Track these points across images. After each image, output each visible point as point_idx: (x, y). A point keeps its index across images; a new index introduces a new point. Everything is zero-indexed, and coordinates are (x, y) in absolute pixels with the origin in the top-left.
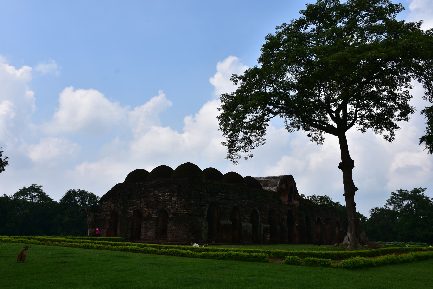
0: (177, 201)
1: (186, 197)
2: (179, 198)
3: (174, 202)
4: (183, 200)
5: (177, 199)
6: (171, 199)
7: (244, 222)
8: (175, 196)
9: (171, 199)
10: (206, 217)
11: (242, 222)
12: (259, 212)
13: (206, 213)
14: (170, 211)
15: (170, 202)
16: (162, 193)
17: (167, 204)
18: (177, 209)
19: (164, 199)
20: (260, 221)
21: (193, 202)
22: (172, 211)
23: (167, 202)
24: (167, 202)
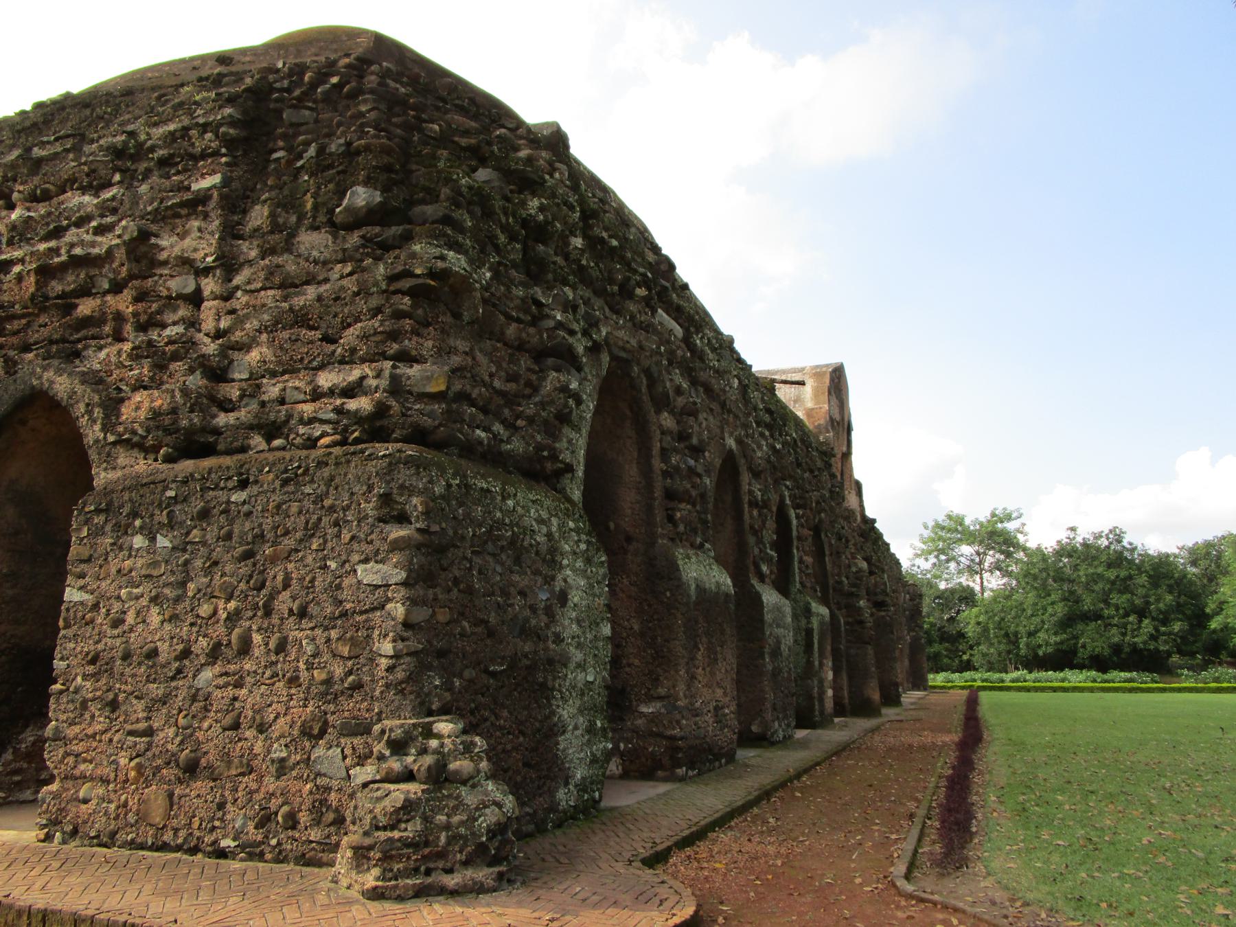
0: (228, 264)
1: (361, 196)
2: (259, 216)
3: (182, 283)
4: (313, 242)
5: (231, 232)
6: (140, 249)
7: (762, 578)
8: (197, 204)
9: (140, 249)
10: (577, 495)
11: (755, 582)
12: (795, 522)
13: (575, 447)
14: (112, 405)
15: (123, 303)
16: (34, 198)
17: (87, 322)
18: (218, 373)
19: (45, 272)
20: (797, 579)
21: (457, 261)
22: (138, 407)
23: (86, 307)
24: (86, 307)
